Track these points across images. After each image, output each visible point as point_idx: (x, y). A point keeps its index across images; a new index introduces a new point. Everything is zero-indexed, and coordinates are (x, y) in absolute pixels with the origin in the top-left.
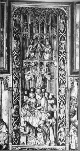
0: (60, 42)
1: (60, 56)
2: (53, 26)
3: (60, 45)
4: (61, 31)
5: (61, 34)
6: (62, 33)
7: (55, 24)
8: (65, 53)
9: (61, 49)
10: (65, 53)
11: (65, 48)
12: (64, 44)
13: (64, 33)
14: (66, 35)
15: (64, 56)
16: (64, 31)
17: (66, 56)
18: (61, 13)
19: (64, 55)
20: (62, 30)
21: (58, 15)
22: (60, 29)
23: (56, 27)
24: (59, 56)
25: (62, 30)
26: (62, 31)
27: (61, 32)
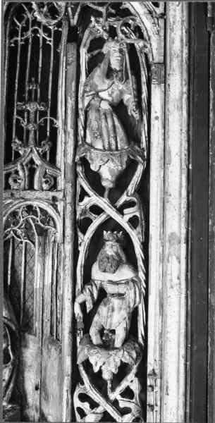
0: (87, 279)
1: (86, 406)
2: (22, 134)
3: (83, 305)
4: (95, 179)
5: (97, 210)
6: (103, 202)
7: (43, 114)
8: (131, 381)
9: (96, 339)
10: (131, 381)
11: (132, 332)
12: (121, 296)
13: (124, 199)
14: (142, 222)
15: (124, 412)
16: (122, 181)
17: (144, 405)
18: (97, 27)
19: (123, 404)
20: (108, 172)
21: (74, 38)
22: (85, 163)
23: (48, 136)
24: (78, 403)
25: (108, 172)
26: (107, 183)
27: (100, 190)
